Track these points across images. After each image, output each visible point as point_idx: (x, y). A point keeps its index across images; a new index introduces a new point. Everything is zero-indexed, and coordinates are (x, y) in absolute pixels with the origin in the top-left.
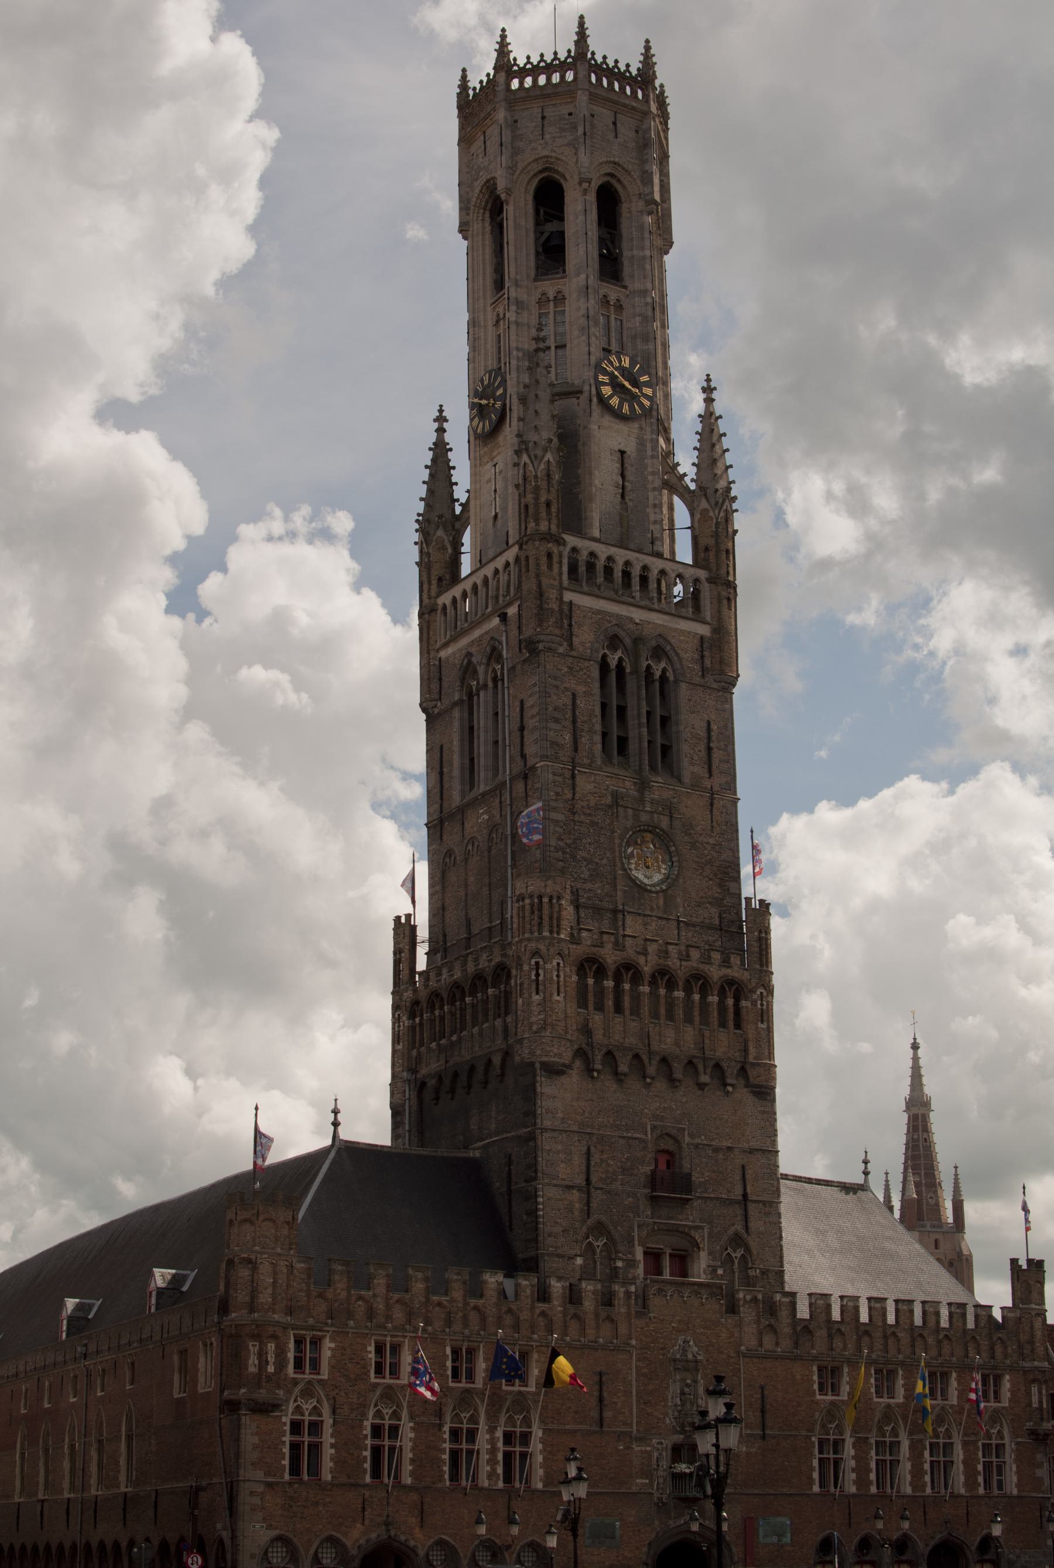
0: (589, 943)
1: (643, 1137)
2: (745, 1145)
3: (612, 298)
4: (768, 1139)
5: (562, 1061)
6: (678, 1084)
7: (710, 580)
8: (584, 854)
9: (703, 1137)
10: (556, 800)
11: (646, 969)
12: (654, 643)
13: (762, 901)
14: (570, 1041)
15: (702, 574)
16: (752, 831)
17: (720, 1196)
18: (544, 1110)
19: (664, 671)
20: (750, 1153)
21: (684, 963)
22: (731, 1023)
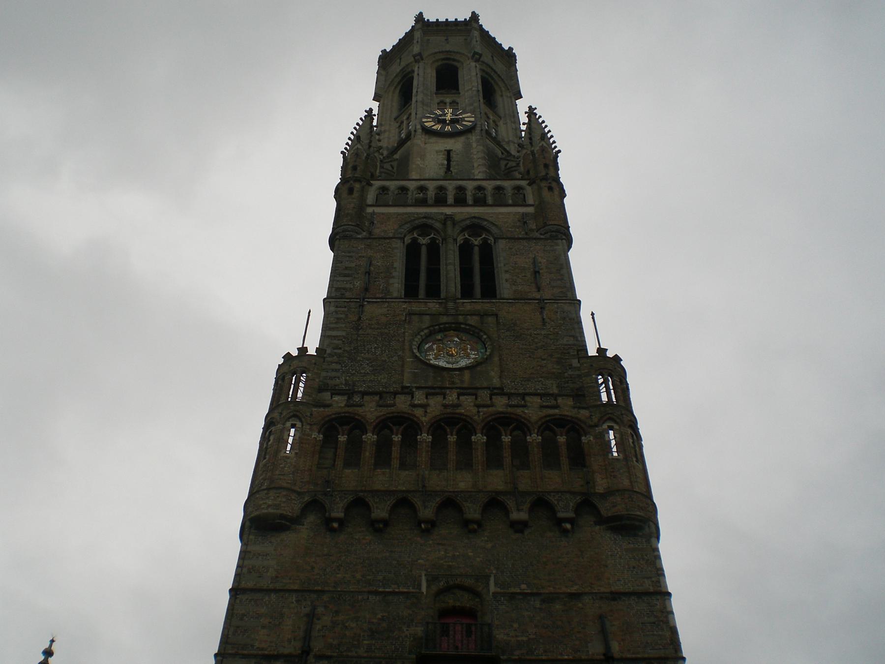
0: (343, 405)
1: (411, 590)
2: (603, 590)
3: (448, 100)
4: (646, 580)
5: (280, 512)
6: (476, 527)
7: (529, 184)
8: (367, 356)
9: (524, 586)
10: (336, 323)
11: (424, 419)
12: (468, 222)
13: (602, 351)
14: (299, 494)
15: (523, 183)
16: (593, 314)
17: (559, 657)
18: (245, 570)
19: (485, 241)
20: (614, 599)
21: (485, 409)
22: (564, 461)
